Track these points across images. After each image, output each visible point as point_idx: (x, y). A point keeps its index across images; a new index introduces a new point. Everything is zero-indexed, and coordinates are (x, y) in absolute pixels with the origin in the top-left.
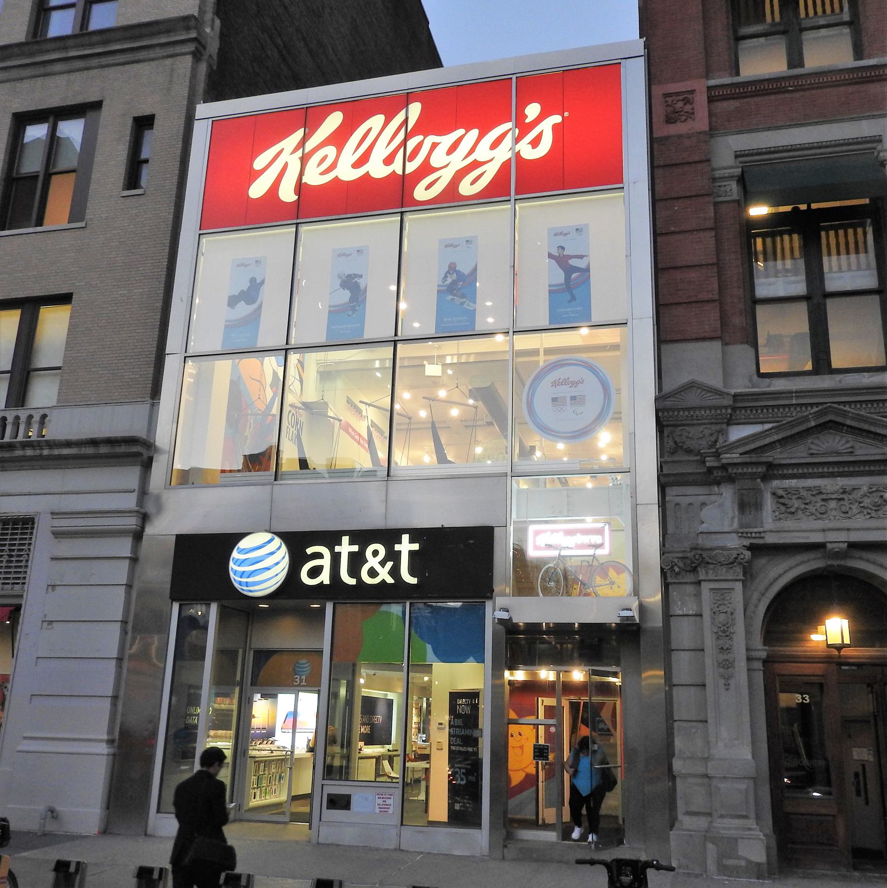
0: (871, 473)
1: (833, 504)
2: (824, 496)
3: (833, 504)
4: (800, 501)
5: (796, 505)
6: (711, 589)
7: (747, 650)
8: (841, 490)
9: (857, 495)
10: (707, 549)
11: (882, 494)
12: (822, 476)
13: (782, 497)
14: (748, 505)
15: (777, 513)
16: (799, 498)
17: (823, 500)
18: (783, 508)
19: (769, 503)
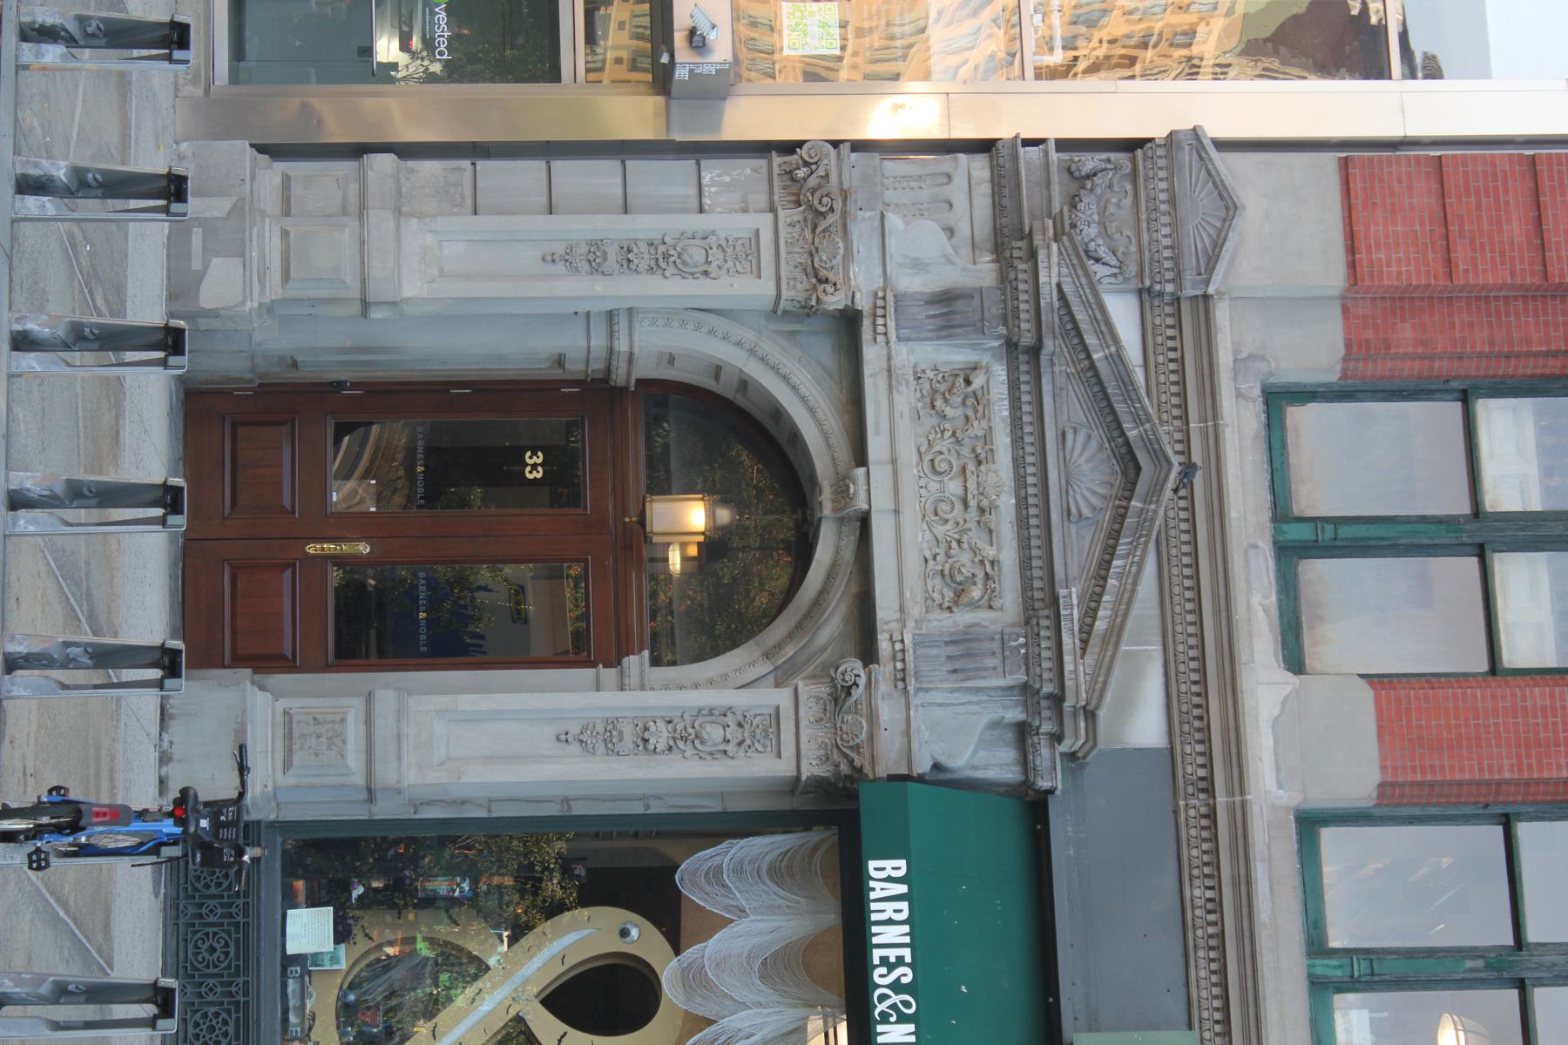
0: (1025, 564)
1: (954, 487)
2: (971, 467)
3: (954, 487)
4: (961, 421)
5: (949, 412)
6: (757, 232)
7: (630, 311)
8: (985, 503)
9: (977, 537)
10: (845, 226)
11: (980, 584)
12: (1018, 463)
13: (968, 382)
14: (949, 312)
15: (930, 374)
16: (967, 418)
17: (964, 469)
18: (943, 387)
19: (953, 355)
